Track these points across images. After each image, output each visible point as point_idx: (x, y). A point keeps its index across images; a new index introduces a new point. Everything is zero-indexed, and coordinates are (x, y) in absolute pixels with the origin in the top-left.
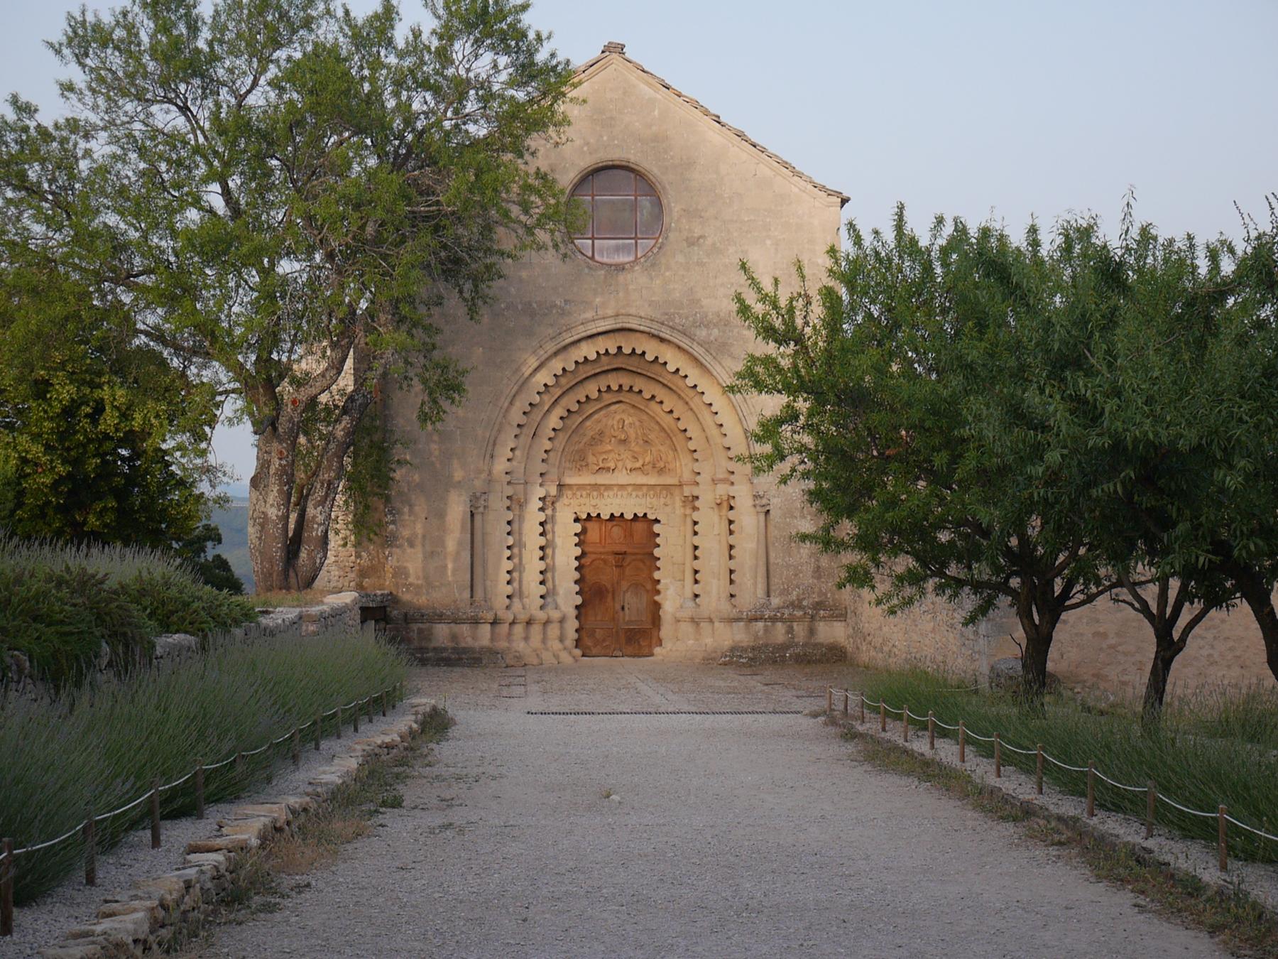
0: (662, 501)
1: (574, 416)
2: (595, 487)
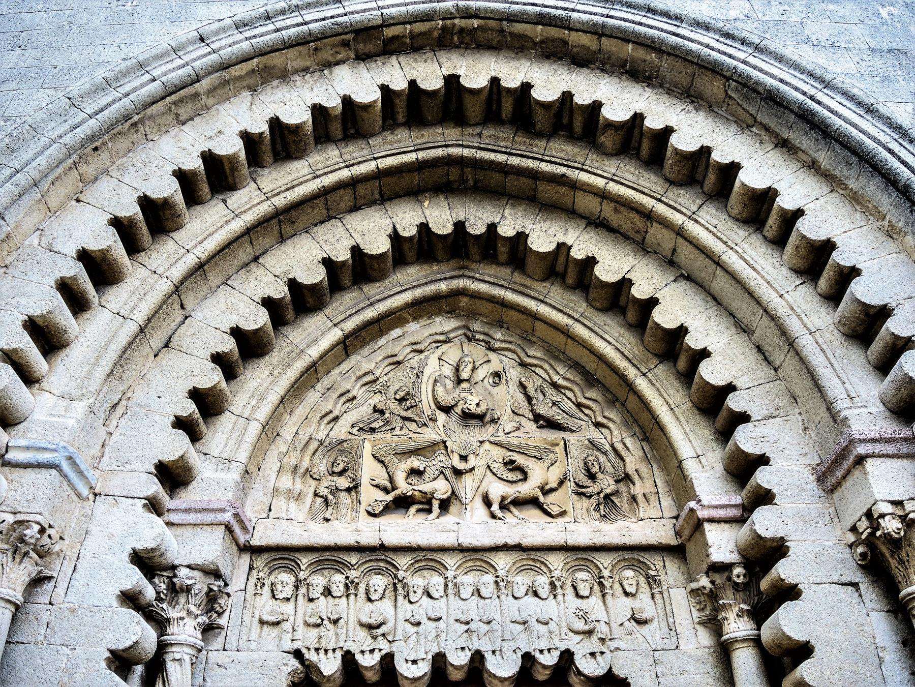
1: (314, 323)
2: (379, 554)
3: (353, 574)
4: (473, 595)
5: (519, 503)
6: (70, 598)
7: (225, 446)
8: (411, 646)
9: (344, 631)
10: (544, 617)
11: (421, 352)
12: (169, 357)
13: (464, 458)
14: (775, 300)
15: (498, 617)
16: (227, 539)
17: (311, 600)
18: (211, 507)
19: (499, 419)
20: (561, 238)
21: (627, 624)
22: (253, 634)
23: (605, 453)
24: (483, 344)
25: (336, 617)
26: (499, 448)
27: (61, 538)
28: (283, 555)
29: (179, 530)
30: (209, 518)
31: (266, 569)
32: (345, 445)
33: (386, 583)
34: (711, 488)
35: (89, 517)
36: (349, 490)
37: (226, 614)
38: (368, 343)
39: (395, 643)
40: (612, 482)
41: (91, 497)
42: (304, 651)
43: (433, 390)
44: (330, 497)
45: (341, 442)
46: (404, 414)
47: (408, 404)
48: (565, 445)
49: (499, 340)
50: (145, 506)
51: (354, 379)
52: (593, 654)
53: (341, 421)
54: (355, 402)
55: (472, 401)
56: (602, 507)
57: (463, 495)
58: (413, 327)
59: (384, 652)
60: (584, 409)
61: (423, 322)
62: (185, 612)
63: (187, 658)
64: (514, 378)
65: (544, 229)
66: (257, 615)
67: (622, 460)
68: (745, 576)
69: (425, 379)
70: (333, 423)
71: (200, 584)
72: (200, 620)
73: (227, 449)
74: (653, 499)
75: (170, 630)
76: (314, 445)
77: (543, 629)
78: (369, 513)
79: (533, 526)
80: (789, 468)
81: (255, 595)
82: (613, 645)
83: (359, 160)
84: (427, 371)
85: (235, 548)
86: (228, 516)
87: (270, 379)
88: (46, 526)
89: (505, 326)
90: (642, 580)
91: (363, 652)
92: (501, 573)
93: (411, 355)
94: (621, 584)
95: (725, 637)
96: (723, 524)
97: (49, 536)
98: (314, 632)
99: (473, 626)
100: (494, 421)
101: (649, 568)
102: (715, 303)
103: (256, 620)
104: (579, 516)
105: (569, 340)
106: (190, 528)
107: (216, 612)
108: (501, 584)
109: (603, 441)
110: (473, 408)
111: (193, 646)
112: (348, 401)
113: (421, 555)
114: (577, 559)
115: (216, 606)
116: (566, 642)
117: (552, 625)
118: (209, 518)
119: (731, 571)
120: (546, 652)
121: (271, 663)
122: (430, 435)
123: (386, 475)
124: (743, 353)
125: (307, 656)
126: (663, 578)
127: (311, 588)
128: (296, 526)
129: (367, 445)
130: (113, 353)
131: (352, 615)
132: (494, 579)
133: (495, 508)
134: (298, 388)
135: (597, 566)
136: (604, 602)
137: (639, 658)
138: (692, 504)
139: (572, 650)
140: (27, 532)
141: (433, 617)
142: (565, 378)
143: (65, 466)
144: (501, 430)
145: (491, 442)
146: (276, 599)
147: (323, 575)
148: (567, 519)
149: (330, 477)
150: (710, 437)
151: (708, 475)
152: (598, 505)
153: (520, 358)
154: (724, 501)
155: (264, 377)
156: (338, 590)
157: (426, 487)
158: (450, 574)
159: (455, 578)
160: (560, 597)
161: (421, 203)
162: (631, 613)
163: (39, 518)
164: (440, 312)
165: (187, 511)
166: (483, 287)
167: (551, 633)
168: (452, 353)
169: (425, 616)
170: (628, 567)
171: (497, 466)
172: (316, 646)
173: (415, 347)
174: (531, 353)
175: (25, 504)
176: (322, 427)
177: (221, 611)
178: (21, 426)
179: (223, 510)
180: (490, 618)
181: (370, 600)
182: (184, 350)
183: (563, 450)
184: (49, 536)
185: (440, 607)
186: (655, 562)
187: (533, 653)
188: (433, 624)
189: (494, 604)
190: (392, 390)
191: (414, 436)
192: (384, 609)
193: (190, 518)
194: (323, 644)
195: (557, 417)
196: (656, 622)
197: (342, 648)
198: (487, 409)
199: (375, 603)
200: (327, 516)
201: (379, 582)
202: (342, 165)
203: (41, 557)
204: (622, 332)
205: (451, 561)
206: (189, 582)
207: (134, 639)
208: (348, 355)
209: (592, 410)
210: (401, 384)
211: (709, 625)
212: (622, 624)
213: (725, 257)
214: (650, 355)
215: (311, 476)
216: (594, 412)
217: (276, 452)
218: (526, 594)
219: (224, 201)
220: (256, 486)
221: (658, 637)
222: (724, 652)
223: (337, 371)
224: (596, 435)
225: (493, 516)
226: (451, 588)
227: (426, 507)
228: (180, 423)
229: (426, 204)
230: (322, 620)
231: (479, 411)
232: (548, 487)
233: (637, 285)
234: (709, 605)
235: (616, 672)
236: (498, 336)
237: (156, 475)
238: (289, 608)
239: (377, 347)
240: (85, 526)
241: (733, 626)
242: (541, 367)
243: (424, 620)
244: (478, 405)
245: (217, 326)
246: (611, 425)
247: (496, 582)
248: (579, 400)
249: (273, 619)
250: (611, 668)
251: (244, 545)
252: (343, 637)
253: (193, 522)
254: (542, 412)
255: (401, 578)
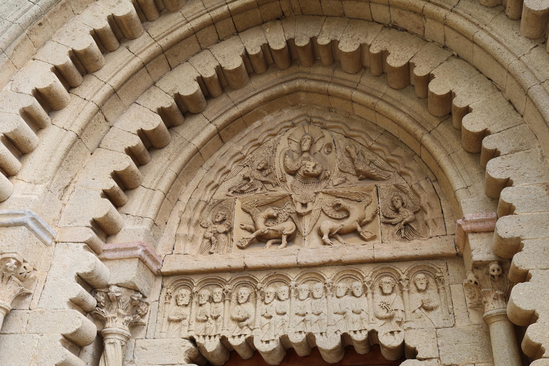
0: (416, 299)
1: (195, 123)
3: (227, 287)
4: (308, 296)
5: (342, 233)
6: (40, 306)
7: (140, 209)
8: (265, 332)
9: (221, 324)
10: (358, 309)
11: (275, 135)
12: (100, 154)
13: (304, 205)
14: (514, 62)
15: (325, 311)
16: (141, 267)
17: (201, 305)
18: (128, 246)
19: (329, 176)
20: (363, 40)
21: (418, 311)
22: (164, 328)
23: (406, 193)
24: (319, 125)
25: (216, 315)
26: (330, 196)
27: (34, 269)
28: (182, 277)
29: (111, 263)
30: (128, 254)
31: (172, 287)
32: (223, 203)
33: (250, 292)
34: (472, 209)
35: (52, 256)
36: (225, 233)
37: (147, 316)
38: (238, 134)
39: (254, 330)
40: (410, 213)
41: (53, 244)
42: (196, 337)
43: (284, 161)
44: (213, 238)
45: (221, 201)
46: (264, 179)
47: (267, 172)
48: (377, 190)
49: (330, 121)
50: (85, 247)
51: (228, 158)
52: (392, 333)
53: (221, 188)
54: (230, 174)
55: (310, 166)
56: (403, 231)
57: (303, 230)
58: (268, 118)
59: (247, 336)
60: (391, 164)
61: (276, 114)
62: (116, 314)
63: (118, 342)
64: (342, 147)
65: (350, 36)
66: (166, 316)
67: (419, 197)
68: (498, 270)
69: (278, 154)
70: (215, 190)
71: (126, 296)
72: (126, 318)
73: (141, 210)
74: (440, 222)
75: (107, 325)
76: (202, 205)
77: (356, 317)
78: (240, 248)
79: (352, 248)
80: (527, 187)
81: (165, 303)
82: (406, 325)
83: (216, 6)
84: (279, 148)
85: (151, 274)
86: (140, 252)
87: (168, 163)
88: (21, 261)
89: (333, 110)
90: (431, 280)
91: (233, 337)
92: (328, 281)
93: (268, 139)
94: (415, 284)
95: (485, 314)
96: (483, 234)
97: (24, 267)
98: (203, 325)
99: (307, 317)
100: (326, 178)
101: (436, 272)
102: (477, 72)
103: (166, 320)
104: (386, 238)
105: (377, 114)
106: (117, 261)
107: (139, 315)
108: (328, 288)
109: (405, 185)
110: (310, 170)
111: (122, 335)
112: (224, 174)
113: (273, 272)
114: (383, 268)
115: (139, 310)
116: (372, 325)
117: (363, 314)
118: (128, 254)
119: (489, 267)
120: (358, 332)
121: (175, 345)
122: (281, 191)
123: (252, 221)
124: (497, 107)
125: (197, 340)
126: (445, 278)
127: (200, 298)
128: (191, 258)
129: (238, 201)
130: (60, 153)
131: (226, 314)
132: (323, 285)
133: (326, 237)
134: (189, 167)
135: (397, 272)
136: (402, 297)
137: (425, 333)
138: (460, 221)
139: (377, 330)
140: (8, 264)
141: (280, 312)
142: (377, 143)
143: (31, 224)
144: (331, 184)
145: (323, 193)
146: (178, 306)
147: (209, 289)
148: (376, 241)
149: (213, 226)
150: (476, 172)
151: (472, 199)
152: (400, 230)
153: (345, 132)
154: (483, 216)
155: (164, 161)
156: (218, 298)
157: (277, 227)
158: (293, 284)
159: (296, 286)
160: (370, 295)
161: (264, 30)
162: (421, 303)
163: (15, 255)
164: (287, 106)
165: (115, 250)
166: (313, 84)
167: (362, 319)
168: (297, 133)
169: (275, 312)
170: (421, 272)
171: (328, 209)
172: (203, 334)
173: (270, 132)
174: (352, 128)
175: (7, 248)
176: (208, 192)
177: (143, 314)
178: (6, 203)
179: (136, 248)
180: (320, 311)
181: (239, 304)
182: (109, 148)
183: (375, 194)
184: (24, 267)
185: (285, 306)
186: (440, 267)
187: (349, 333)
188: (280, 317)
189: (322, 302)
190: (256, 163)
191: (269, 193)
192: (249, 308)
193: (116, 255)
194: (208, 333)
195: (372, 171)
196: (439, 310)
197: (220, 334)
198: (322, 171)
199: (242, 305)
200: (211, 250)
201: (245, 291)
202: (204, 11)
203: (22, 281)
204: (413, 103)
205: (293, 276)
206: (117, 295)
207: (77, 327)
208: (224, 143)
209: (397, 163)
210: (262, 159)
211: (479, 309)
212: (414, 312)
213: (477, 36)
214: (433, 118)
215: (201, 226)
216: (399, 165)
217: (177, 211)
218: (346, 294)
219: (128, 48)
220: (164, 234)
221: (440, 319)
222: (486, 325)
223: (217, 154)
224: (400, 181)
225: (325, 243)
226: (294, 293)
227: (278, 240)
228: (106, 194)
229: (267, 30)
230: (208, 317)
231: (316, 171)
232: (365, 220)
233: (418, 66)
234: (477, 293)
235: (408, 343)
236: (329, 118)
237: (92, 228)
238: (186, 311)
239: (244, 135)
240: (50, 261)
241: (491, 306)
242: (360, 136)
243: (274, 315)
244: (314, 167)
245: (129, 131)
246: (410, 173)
247: (325, 288)
248: (387, 157)
249: (176, 318)
250: (404, 341)
251: (157, 272)
252: (220, 328)
253: (119, 257)
254: (360, 168)
255: (259, 288)
